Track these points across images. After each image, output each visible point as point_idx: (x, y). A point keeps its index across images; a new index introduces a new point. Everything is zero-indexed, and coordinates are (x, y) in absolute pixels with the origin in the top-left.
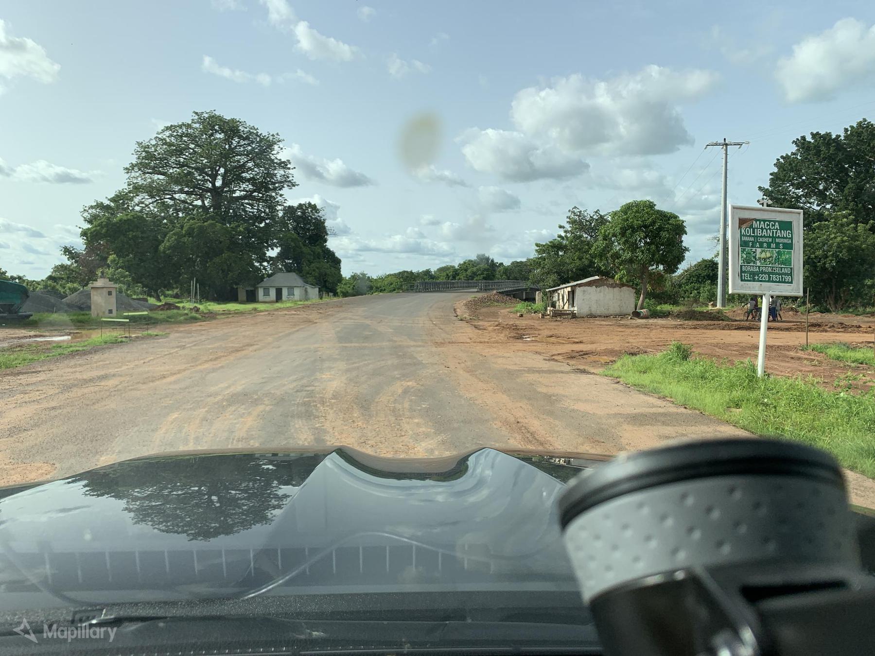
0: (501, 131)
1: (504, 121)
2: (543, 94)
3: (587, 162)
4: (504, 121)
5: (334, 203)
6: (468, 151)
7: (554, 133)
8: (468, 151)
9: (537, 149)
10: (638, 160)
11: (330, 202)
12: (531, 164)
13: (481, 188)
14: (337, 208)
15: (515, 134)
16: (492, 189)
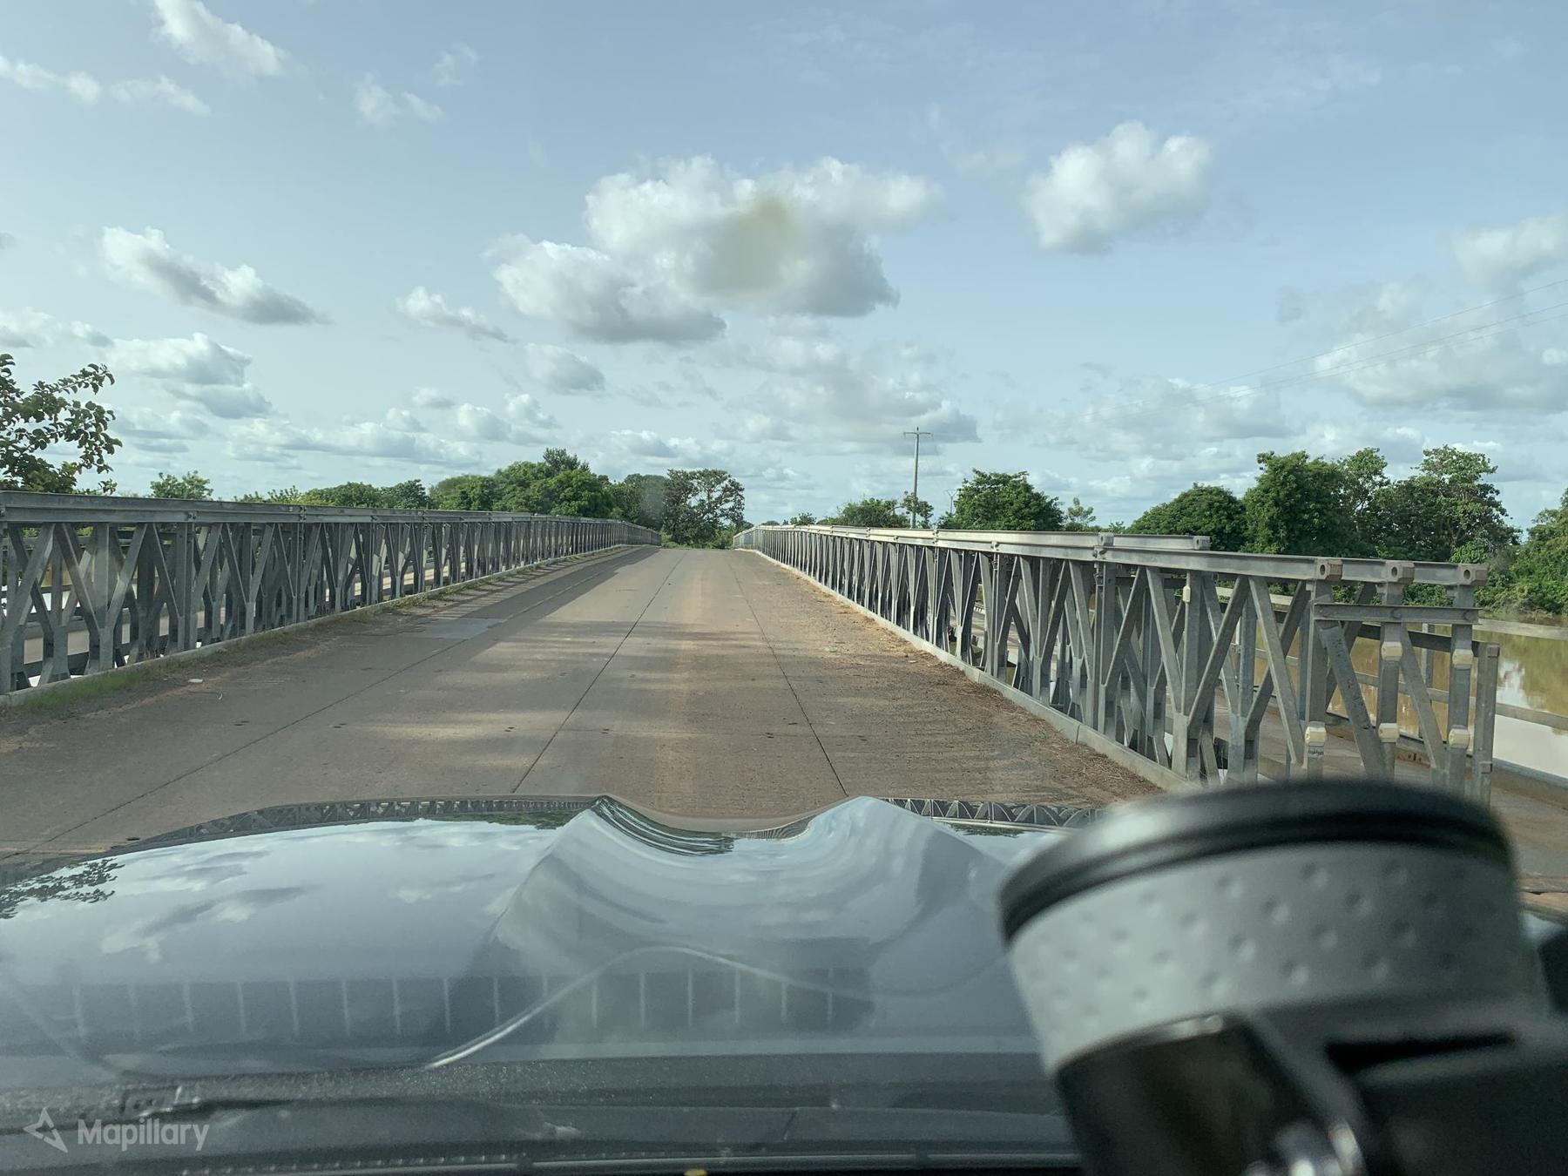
0: (568, 247)
1: (573, 229)
2: (647, 187)
3: (721, 316)
4: (573, 229)
5: (240, 353)
6: (508, 276)
7: (665, 260)
8: (508, 276)
9: (633, 285)
10: (806, 322)
11: (230, 350)
12: (623, 312)
13: (530, 347)
14: (245, 362)
15: (592, 254)
16: (549, 349)
